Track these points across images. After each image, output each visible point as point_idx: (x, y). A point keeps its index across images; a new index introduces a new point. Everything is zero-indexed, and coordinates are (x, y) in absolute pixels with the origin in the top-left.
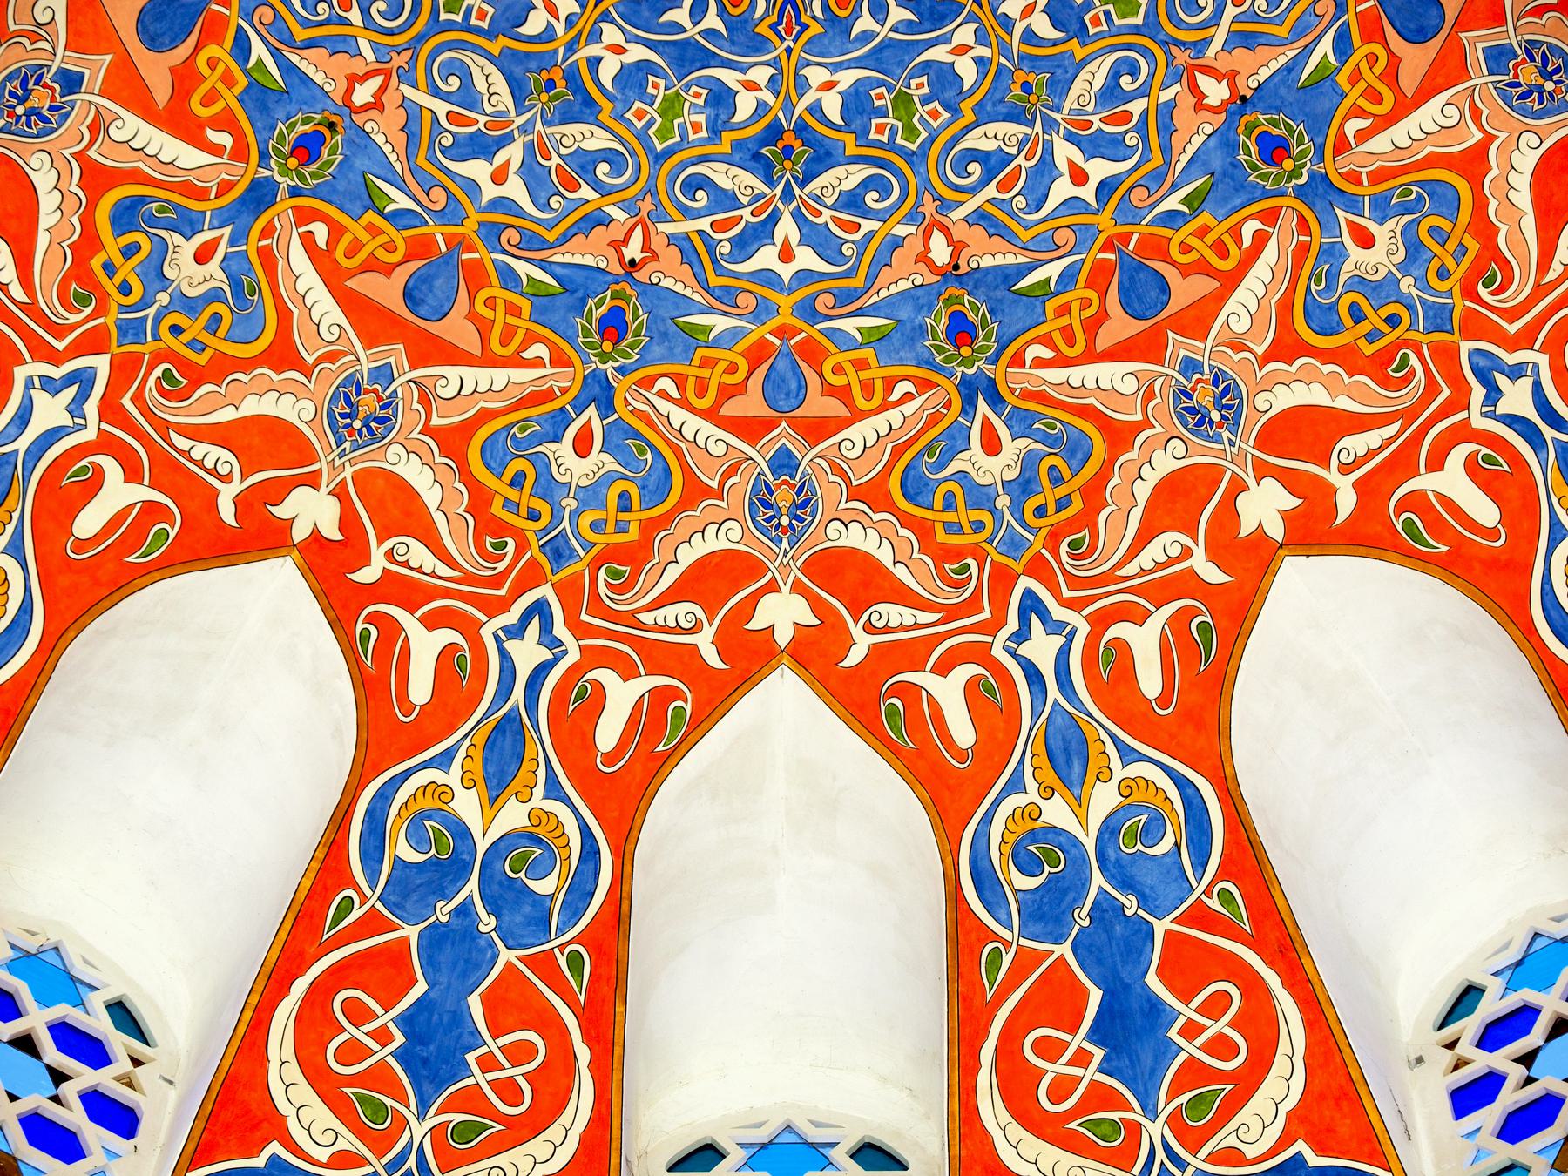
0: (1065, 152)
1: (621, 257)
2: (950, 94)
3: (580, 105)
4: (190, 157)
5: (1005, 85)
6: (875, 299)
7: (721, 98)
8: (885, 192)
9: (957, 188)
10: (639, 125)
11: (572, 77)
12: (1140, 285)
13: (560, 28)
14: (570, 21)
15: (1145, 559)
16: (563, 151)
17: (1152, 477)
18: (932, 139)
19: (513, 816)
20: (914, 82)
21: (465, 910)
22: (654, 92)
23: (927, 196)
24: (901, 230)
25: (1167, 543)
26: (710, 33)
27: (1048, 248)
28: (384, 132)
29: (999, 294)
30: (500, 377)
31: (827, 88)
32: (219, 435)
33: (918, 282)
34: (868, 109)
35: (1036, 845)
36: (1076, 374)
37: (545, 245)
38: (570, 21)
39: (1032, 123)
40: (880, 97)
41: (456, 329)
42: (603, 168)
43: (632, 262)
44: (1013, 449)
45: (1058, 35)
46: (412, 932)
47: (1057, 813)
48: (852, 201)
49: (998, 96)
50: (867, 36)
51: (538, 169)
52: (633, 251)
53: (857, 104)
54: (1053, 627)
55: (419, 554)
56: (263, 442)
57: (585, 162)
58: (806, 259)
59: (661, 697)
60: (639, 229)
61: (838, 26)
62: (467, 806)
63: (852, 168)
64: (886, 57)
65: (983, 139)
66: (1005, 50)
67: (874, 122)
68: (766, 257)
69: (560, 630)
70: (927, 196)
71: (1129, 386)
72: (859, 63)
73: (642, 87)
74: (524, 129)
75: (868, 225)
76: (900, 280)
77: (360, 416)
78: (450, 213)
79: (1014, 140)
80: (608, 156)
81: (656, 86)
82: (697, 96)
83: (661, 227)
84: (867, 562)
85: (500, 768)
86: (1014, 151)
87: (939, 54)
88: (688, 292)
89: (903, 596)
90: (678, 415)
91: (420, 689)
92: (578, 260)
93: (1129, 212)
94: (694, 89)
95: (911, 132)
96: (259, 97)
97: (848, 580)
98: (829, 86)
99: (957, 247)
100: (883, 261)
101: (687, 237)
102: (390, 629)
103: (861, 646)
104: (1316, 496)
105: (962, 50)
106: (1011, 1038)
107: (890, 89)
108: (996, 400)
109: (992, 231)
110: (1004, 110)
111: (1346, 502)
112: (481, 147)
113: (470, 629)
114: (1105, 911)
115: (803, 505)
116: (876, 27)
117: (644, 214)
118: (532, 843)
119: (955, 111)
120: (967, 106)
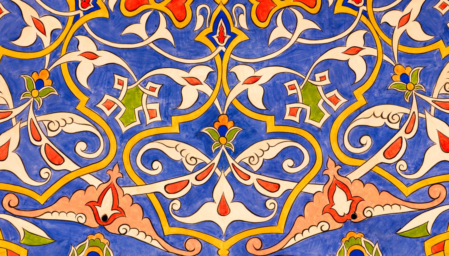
1: (96, 214)
2: (345, 85)
3: (64, 101)
5: (388, 77)
6: (292, 242)
7: (171, 91)
8: (298, 159)
9: (353, 156)
10: (108, 113)
11: (56, 77)
13: (46, 40)
14: (54, 35)
16: (51, 134)
18: (333, 119)
20: (318, 76)
22: (120, 87)
23: (331, 162)
24: (311, 189)
26: (161, 42)
27: (424, 197)
29: (388, 236)
31: (252, 82)
33: (326, 228)
34: (284, 97)
37: (36, 206)
38: (54, 35)
39: (409, 105)
40: (292, 87)
42: (81, 147)
43: (105, 218)
45: (427, 38)
48: (273, 167)
49: (383, 85)
50: (281, 42)
51: (31, 148)
52: (105, 209)
53: (275, 94)
57: (67, 142)
58: (239, 212)
60: (109, 192)
61: (259, 36)
63: (272, 142)
64: (298, 58)
65: (374, 117)
66: (387, 50)
67: (288, 107)
68: (208, 212)
70: (331, 162)
72: (275, 62)
73: (111, 83)
74: (19, 118)
75: (285, 185)
79: (396, 118)
80: (85, 136)
81: (121, 83)
82: (153, 89)
83: (127, 190)
86: (396, 126)
87: (337, 54)
88: (148, 240)
92: (63, 217)
94: (150, 84)
95: (317, 113)
98: (254, 80)
100: (298, 212)
101: (146, 198)
105: (355, 50)
107: (300, 81)
109: (381, 188)
110: (388, 96)
116: (288, 35)
117: (113, 180)
119: (351, 98)
120: (359, 93)
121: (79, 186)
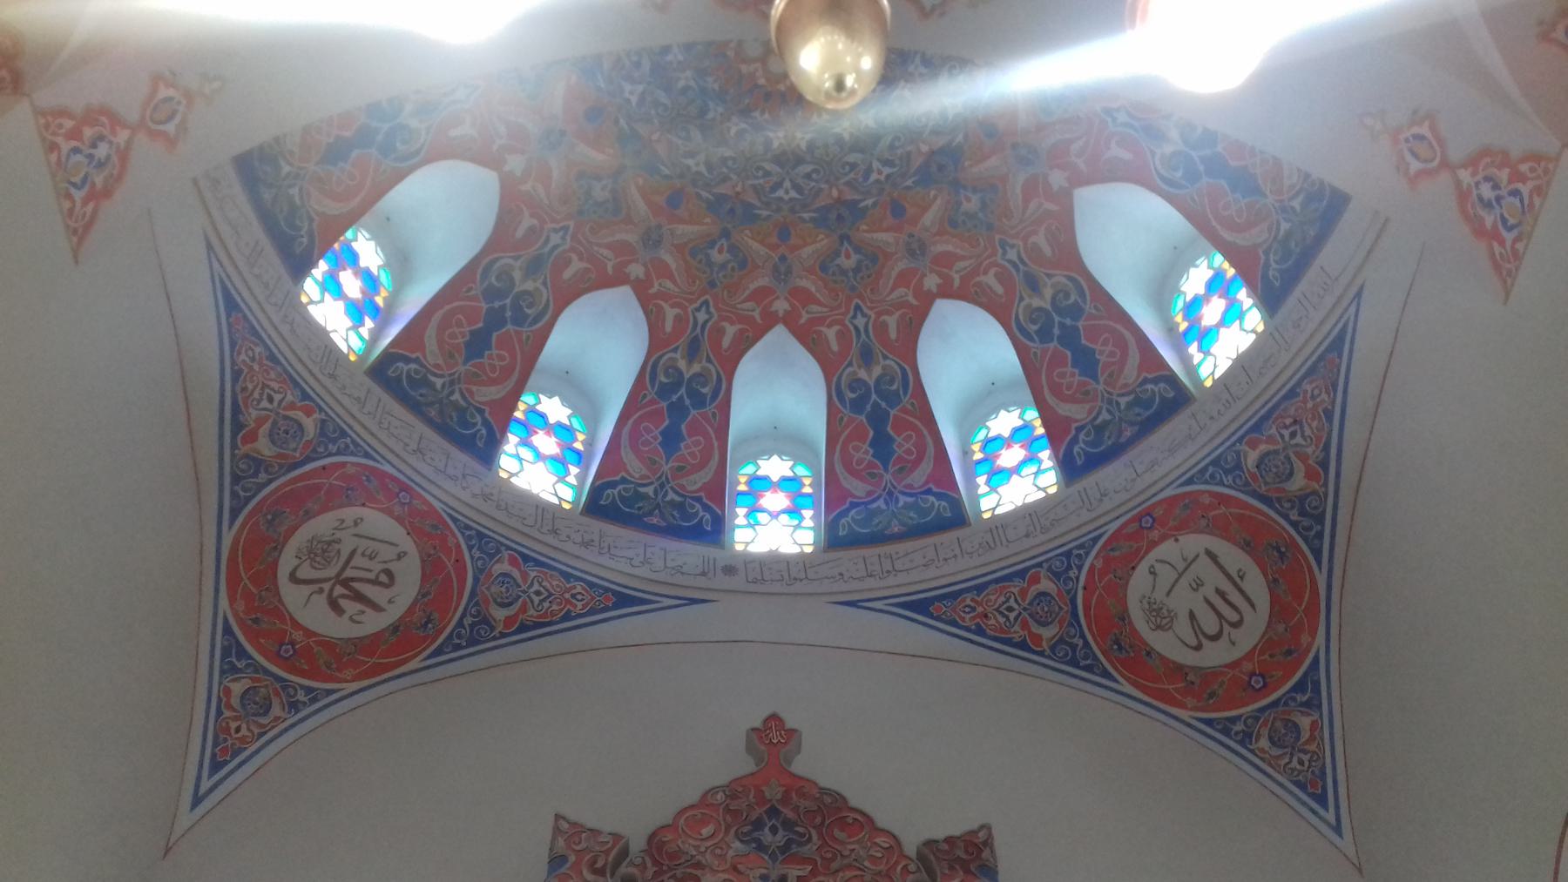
15: (894, 296)
17: (897, 270)
19: (696, 368)
21: (681, 399)
25: (902, 291)
30: (696, 228)
32: (609, 246)
35: (856, 384)
36: (875, 235)
44: (855, 258)
46: (664, 404)
47: (862, 374)
48: (808, 176)
52: (739, 189)
54: (864, 315)
55: (669, 284)
58: (793, 194)
59: (741, 332)
62: (682, 364)
68: (780, 193)
69: (712, 310)
71: (891, 240)
76: (821, 202)
84: (805, 291)
85: (693, 350)
89: (819, 303)
90: (750, 242)
91: (669, 326)
97: (802, 297)
99: (840, 192)
102: (660, 309)
103: (805, 317)
104: (948, 281)
106: (845, 444)
108: (850, 242)
111: (957, 283)
113: (684, 308)
114: (876, 405)
115: (789, 272)
118: (701, 377)
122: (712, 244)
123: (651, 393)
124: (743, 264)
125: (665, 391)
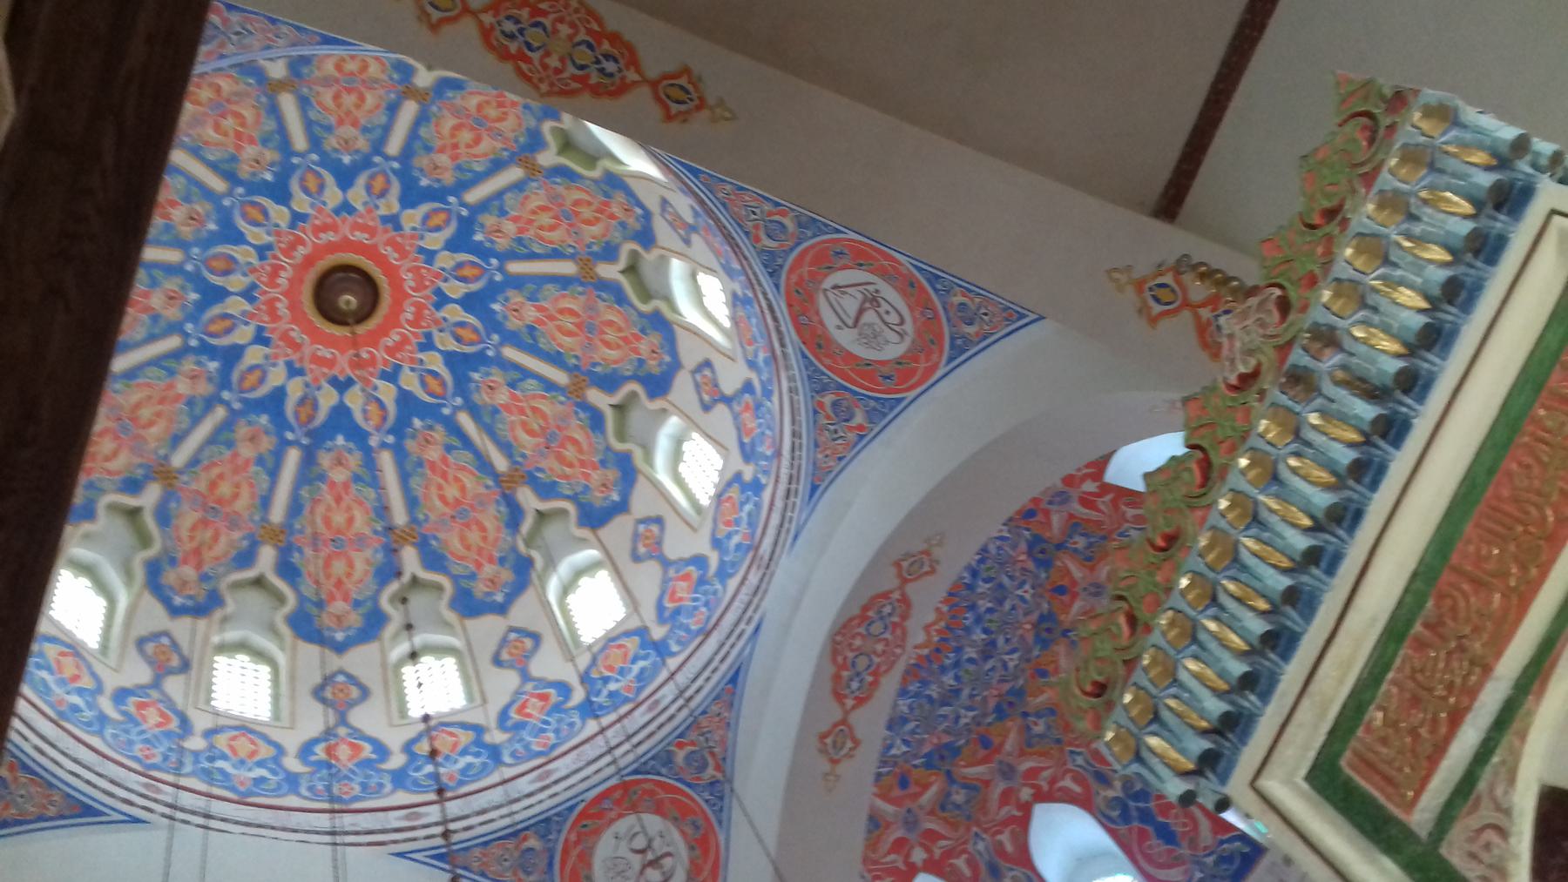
0: (1019, 592)
3: (956, 692)
4: (934, 789)
7: (971, 660)
12: (1061, 590)
19: (1118, 784)
27: (1039, 605)
28: (946, 739)
31: (978, 636)
41: (996, 741)
48: (1007, 640)
53: (986, 631)
55: (1046, 774)
56: (1006, 797)
57: (972, 696)
58: (1015, 656)
62: (1111, 793)
64: (978, 620)
68: (1011, 665)
76: (1030, 638)
77: (1008, 772)
78: (970, 731)
93: (1040, 585)
96: (928, 765)
102: (1060, 789)
112: (958, 718)
121: (985, 699)
122: (1028, 728)
123: (1123, 829)
124: (1052, 712)
125: (1125, 817)
